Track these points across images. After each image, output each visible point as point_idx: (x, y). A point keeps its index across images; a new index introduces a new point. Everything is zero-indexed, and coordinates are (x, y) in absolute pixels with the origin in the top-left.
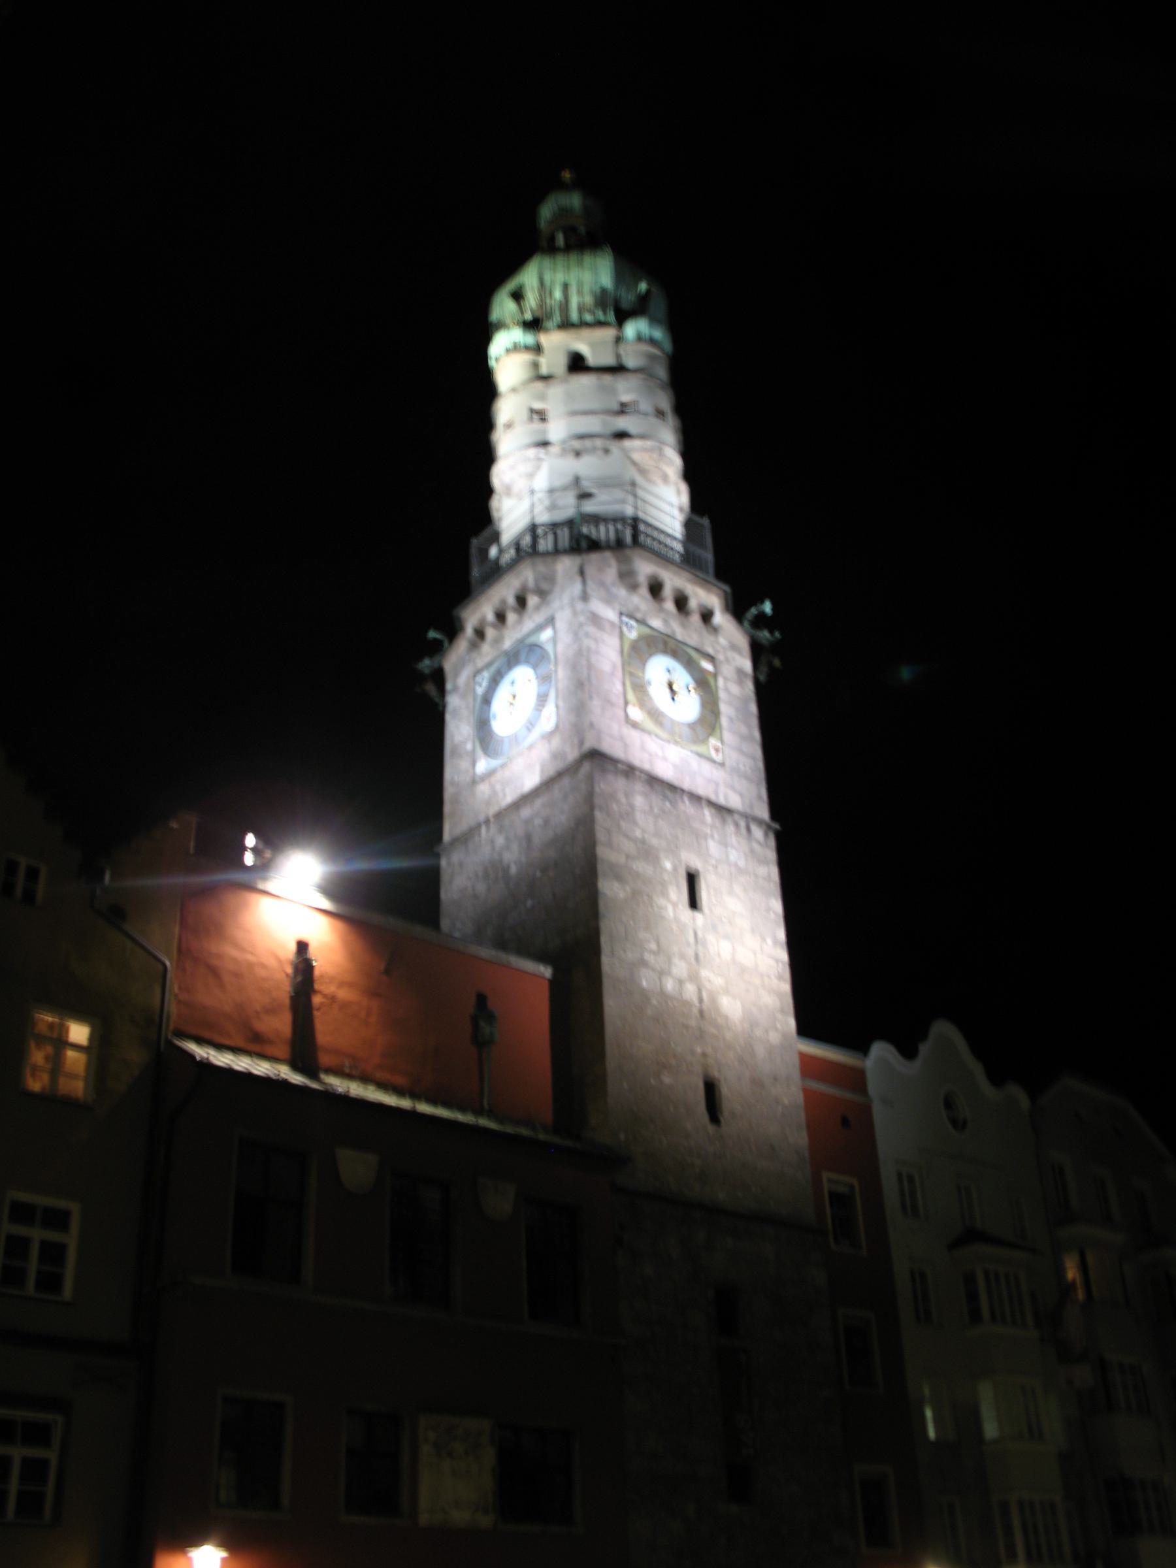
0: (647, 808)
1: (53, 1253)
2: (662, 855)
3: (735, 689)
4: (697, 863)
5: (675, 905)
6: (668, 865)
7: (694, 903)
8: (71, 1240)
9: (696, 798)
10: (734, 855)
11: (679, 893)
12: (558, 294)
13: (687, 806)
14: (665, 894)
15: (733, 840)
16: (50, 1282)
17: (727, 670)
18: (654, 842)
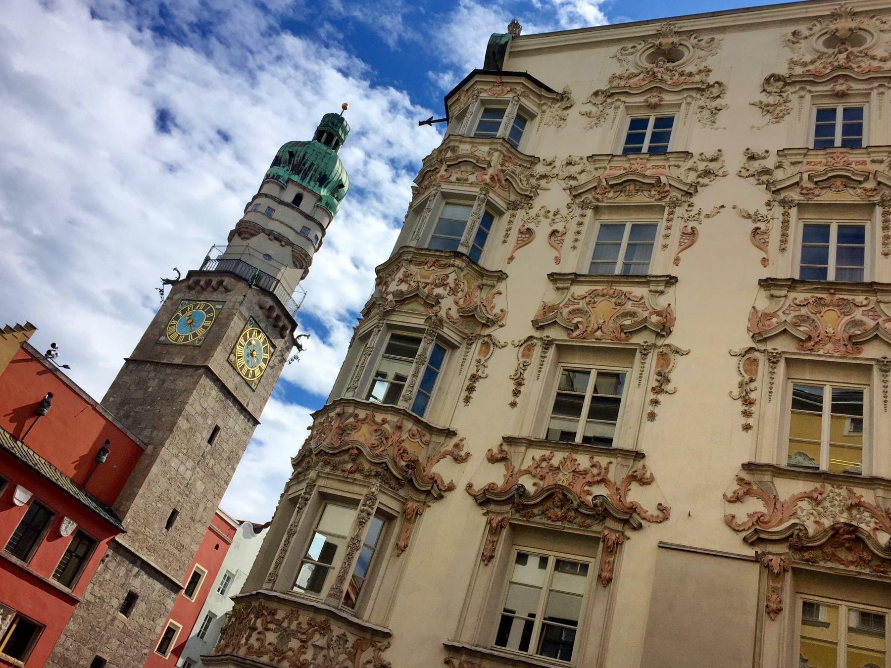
4: (221, 425)
5: (203, 438)
7: (210, 441)
11: (207, 435)
12: (307, 166)
14: (201, 433)
15: (240, 422)
18: (210, 411)
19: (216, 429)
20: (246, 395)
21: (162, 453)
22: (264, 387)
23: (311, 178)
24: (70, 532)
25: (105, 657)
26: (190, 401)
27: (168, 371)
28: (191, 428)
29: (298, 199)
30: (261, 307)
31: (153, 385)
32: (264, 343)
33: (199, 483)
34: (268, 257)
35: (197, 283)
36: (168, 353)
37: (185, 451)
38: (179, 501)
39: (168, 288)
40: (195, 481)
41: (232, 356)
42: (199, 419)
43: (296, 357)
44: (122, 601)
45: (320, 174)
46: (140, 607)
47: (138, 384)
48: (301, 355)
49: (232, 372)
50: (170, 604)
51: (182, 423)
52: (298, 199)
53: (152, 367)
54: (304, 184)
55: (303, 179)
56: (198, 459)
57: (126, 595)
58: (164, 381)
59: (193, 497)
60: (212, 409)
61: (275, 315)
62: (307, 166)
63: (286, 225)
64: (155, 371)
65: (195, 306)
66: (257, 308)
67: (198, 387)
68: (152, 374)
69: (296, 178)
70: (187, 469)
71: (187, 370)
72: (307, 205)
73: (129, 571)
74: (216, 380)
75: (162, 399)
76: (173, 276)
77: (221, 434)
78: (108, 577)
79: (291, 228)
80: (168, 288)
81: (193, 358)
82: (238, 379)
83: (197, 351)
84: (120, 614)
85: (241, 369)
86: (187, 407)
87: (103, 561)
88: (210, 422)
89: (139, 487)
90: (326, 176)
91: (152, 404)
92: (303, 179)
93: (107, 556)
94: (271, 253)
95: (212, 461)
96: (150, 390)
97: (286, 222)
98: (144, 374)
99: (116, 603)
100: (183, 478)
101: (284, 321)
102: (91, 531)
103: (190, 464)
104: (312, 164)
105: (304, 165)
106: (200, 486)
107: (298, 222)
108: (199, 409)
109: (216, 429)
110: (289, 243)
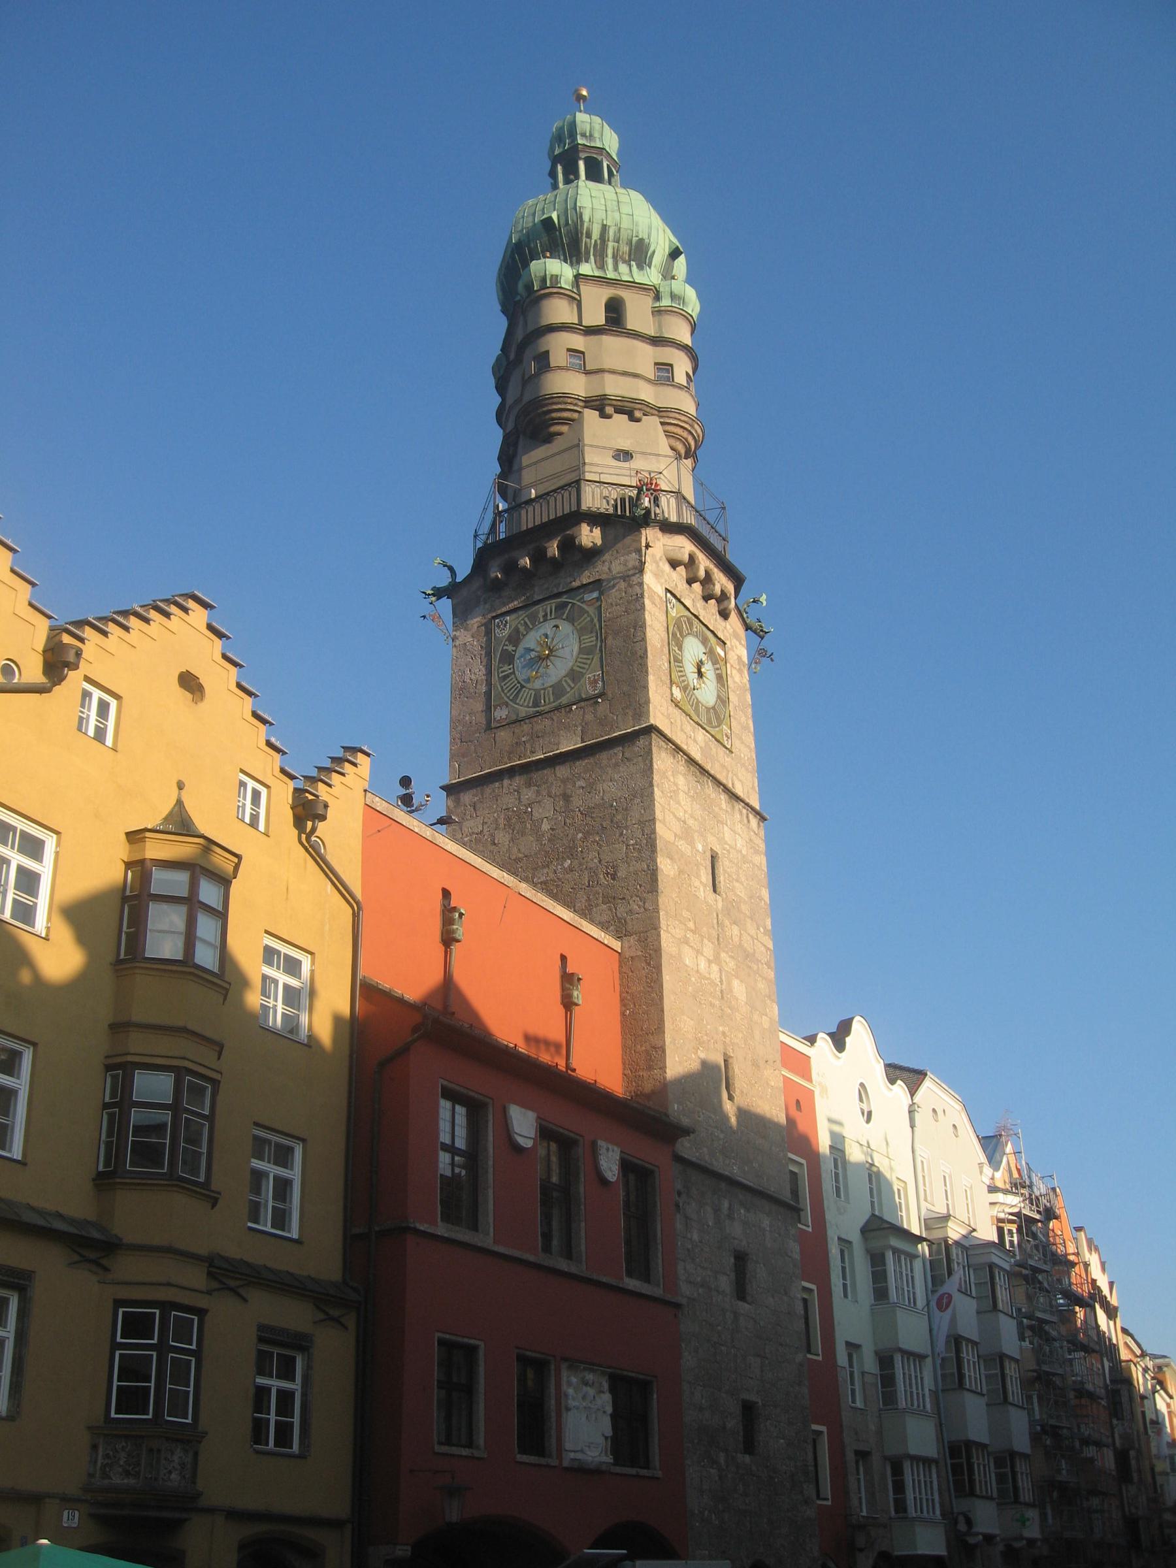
0: (686, 789)
1: (283, 1186)
2: (696, 835)
3: (737, 678)
5: (705, 886)
6: (700, 847)
8: (295, 1174)
9: (718, 783)
10: (740, 843)
11: (706, 877)
12: (596, 235)
13: (710, 789)
14: (698, 876)
15: (738, 827)
16: (281, 1219)
17: (732, 658)
18: (691, 822)
19: (714, 858)
20: (723, 766)
21: (664, 944)
22: (740, 739)
23: (615, 257)
24: (615, 1168)
25: (753, 1397)
26: (658, 814)
27: (562, 771)
28: (681, 872)
29: (615, 310)
30: (674, 564)
31: (545, 813)
32: (704, 641)
33: (736, 983)
34: (624, 455)
35: (511, 568)
36: (535, 736)
37: (691, 925)
38: (724, 1033)
39: (446, 605)
40: (729, 983)
41: (674, 687)
42: (682, 845)
43: (762, 653)
44: (733, 1276)
45: (630, 242)
46: (759, 1274)
47: (509, 825)
48: (765, 643)
49: (689, 726)
50: (795, 1248)
51: (665, 866)
52: (615, 310)
53: (518, 781)
54: (611, 274)
55: (601, 266)
56: (714, 934)
57: (732, 1260)
58: (566, 798)
59: (738, 1016)
60: (692, 816)
61: (702, 574)
62: (596, 235)
63: (625, 374)
64: (529, 785)
65: (533, 618)
66: (667, 567)
67: (656, 778)
68: (528, 794)
69: (586, 269)
70: (710, 962)
71: (604, 756)
72: (638, 315)
73: (717, 1210)
74: (678, 749)
75: (587, 835)
76: (444, 580)
77: (723, 865)
78: (696, 1237)
79: (636, 376)
80: (446, 605)
81: (603, 722)
82: (701, 735)
83: (603, 707)
84: (740, 1303)
85: (697, 711)
86: (659, 828)
87: (677, 1206)
88: (700, 847)
89: (660, 1029)
90: (641, 241)
91: (571, 852)
92: (601, 266)
93: (679, 1194)
94: (625, 445)
95: (735, 930)
96: (545, 826)
97: (620, 368)
98: (510, 801)
99: (725, 1283)
100: (713, 983)
101: (722, 582)
102: (649, 1153)
103: (708, 949)
104: (604, 228)
105: (589, 236)
106: (739, 989)
107: (644, 357)
108: (676, 827)
109: (714, 858)
110: (651, 410)
